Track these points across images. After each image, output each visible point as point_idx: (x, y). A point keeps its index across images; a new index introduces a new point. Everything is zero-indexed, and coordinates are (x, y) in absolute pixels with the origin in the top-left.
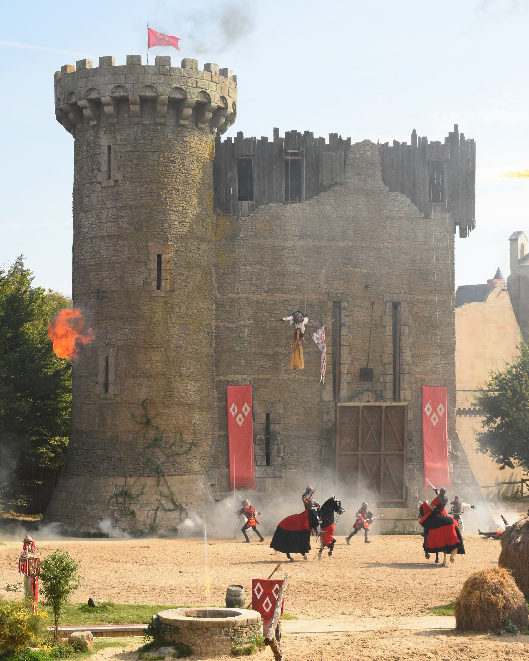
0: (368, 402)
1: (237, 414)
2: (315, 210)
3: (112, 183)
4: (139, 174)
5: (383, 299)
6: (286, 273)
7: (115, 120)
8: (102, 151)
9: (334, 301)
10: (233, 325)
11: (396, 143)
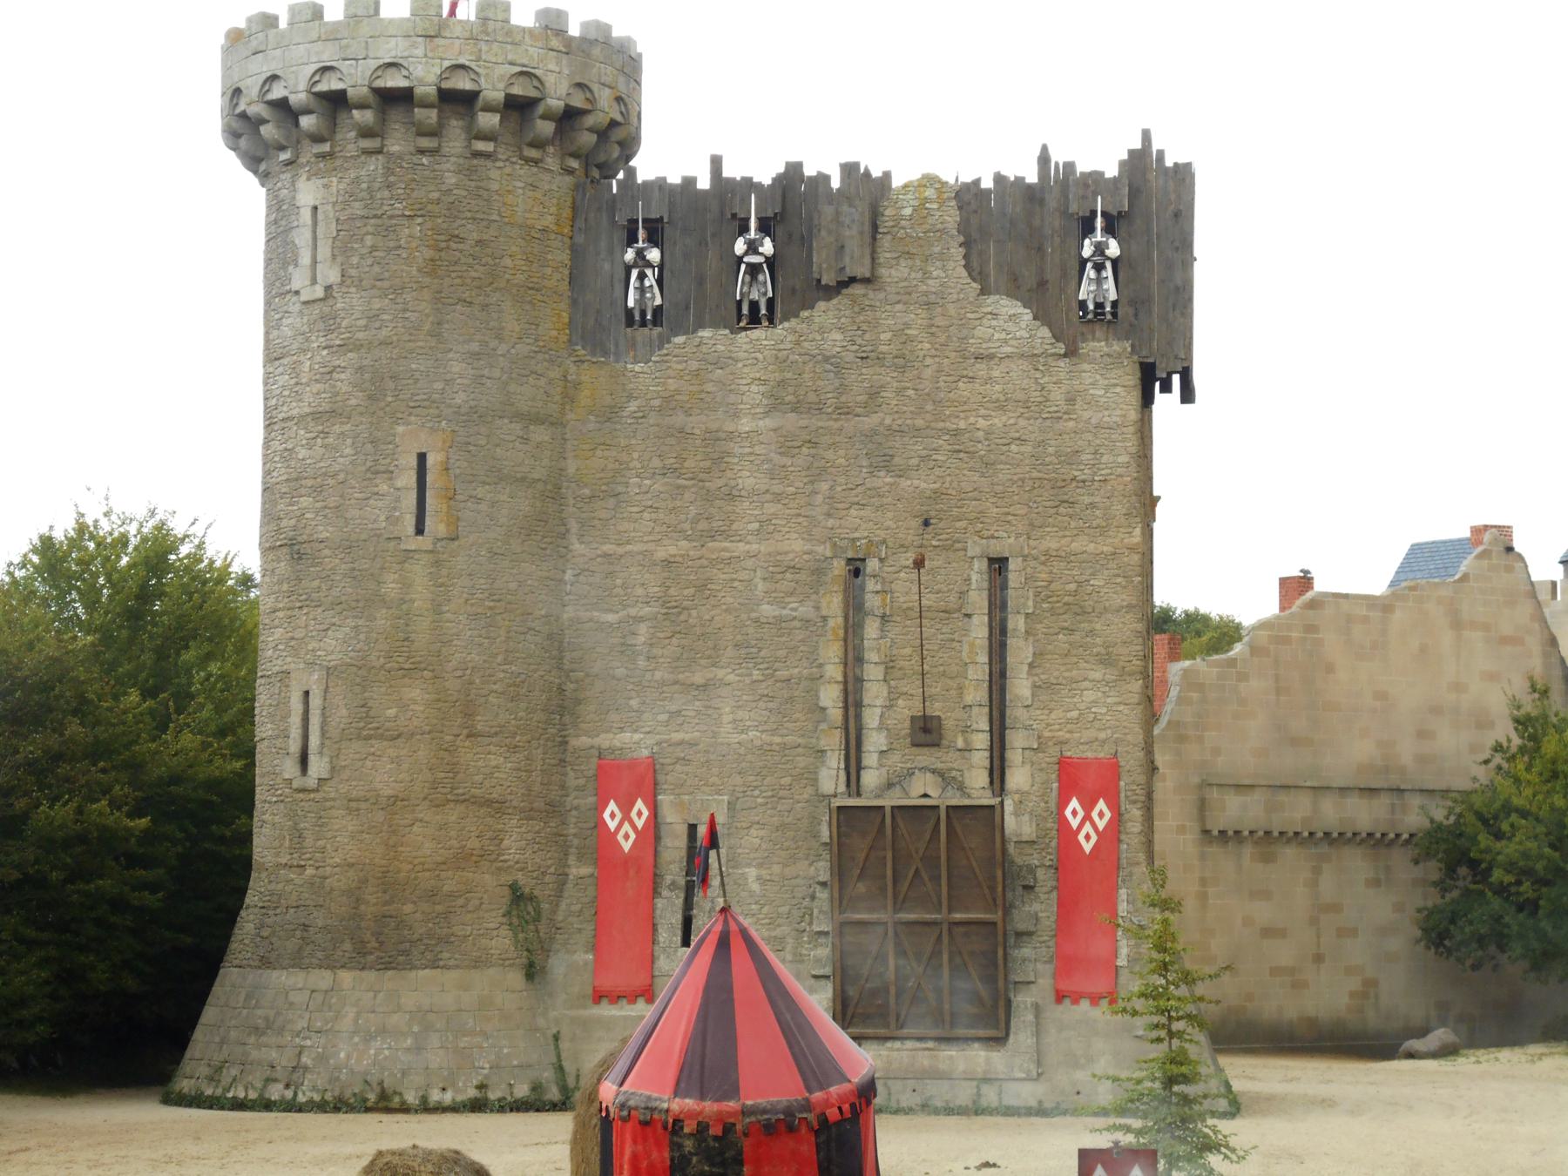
0: (925, 795)
1: (619, 828)
2: (806, 344)
3: (319, 292)
4: (377, 269)
5: (966, 550)
6: (735, 492)
7: (326, 147)
8: (301, 221)
9: (849, 557)
10: (611, 617)
11: (999, 179)
